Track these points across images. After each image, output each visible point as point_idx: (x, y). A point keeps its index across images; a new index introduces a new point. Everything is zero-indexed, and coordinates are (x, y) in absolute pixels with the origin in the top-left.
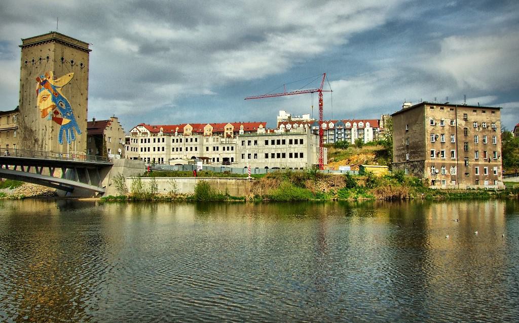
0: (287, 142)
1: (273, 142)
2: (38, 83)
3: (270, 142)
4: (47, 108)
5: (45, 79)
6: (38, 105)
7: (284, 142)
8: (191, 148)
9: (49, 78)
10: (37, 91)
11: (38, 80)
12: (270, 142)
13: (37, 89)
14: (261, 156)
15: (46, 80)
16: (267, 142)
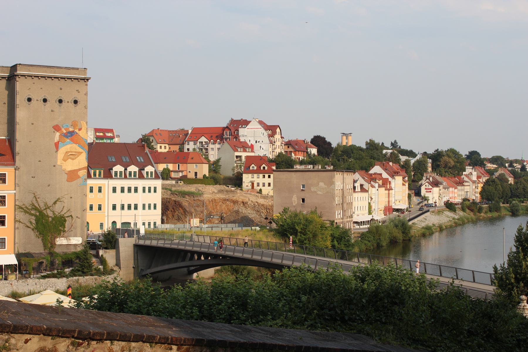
0: (140, 190)
1: (123, 190)
2: (58, 134)
3: (118, 190)
4: (80, 170)
5: (71, 129)
6: (59, 163)
7: (136, 190)
9: (80, 130)
10: (57, 145)
11: (57, 128)
12: (118, 190)
13: (56, 141)
14: (107, 207)
15: (73, 132)
16: (114, 190)
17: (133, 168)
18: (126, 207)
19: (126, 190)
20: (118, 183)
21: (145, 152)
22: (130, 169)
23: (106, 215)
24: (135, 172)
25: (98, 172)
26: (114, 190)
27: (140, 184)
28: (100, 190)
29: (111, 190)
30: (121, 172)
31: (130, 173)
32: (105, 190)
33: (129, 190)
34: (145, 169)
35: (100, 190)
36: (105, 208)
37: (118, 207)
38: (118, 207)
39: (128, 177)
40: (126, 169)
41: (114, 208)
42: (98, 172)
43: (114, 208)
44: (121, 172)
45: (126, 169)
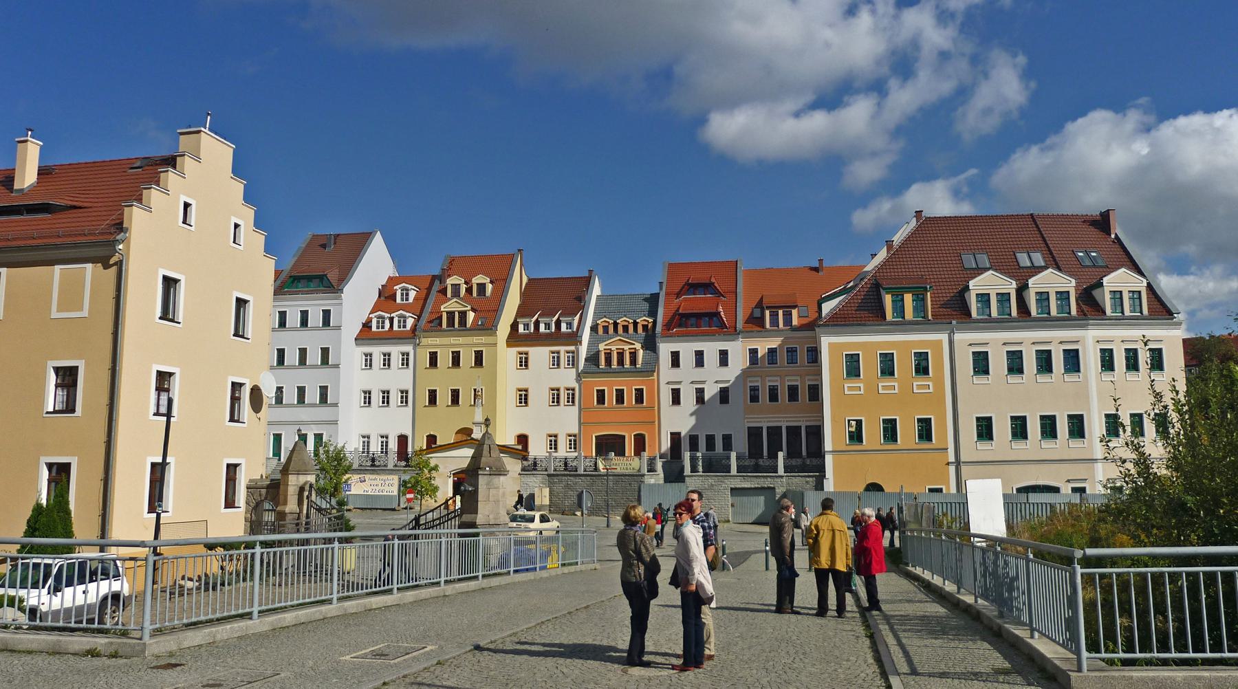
0: (1091, 360)
1: (1015, 364)
3: (998, 363)
7: (1073, 360)
8: (455, 395)
12: (998, 363)
16: (981, 364)
17: (1050, 281)
18: (1034, 427)
19: (1030, 363)
20: (996, 342)
21: (1113, 236)
22: (1036, 284)
23: (952, 458)
24: (1063, 296)
25: (908, 298)
26: (981, 364)
27: (1090, 340)
28: (922, 368)
29: (965, 364)
30: (1003, 298)
31: (1043, 298)
32: (940, 365)
33: (1045, 361)
34: (1105, 280)
35: (922, 368)
36: (943, 433)
37: (1002, 429)
38: (1002, 429)
39: (1034, 312)
40: (1022, 289)
41: (985, 429)
42: (908, 298)
43: (985, 429)
44: (1003, 298)
45: (1022, 289)
